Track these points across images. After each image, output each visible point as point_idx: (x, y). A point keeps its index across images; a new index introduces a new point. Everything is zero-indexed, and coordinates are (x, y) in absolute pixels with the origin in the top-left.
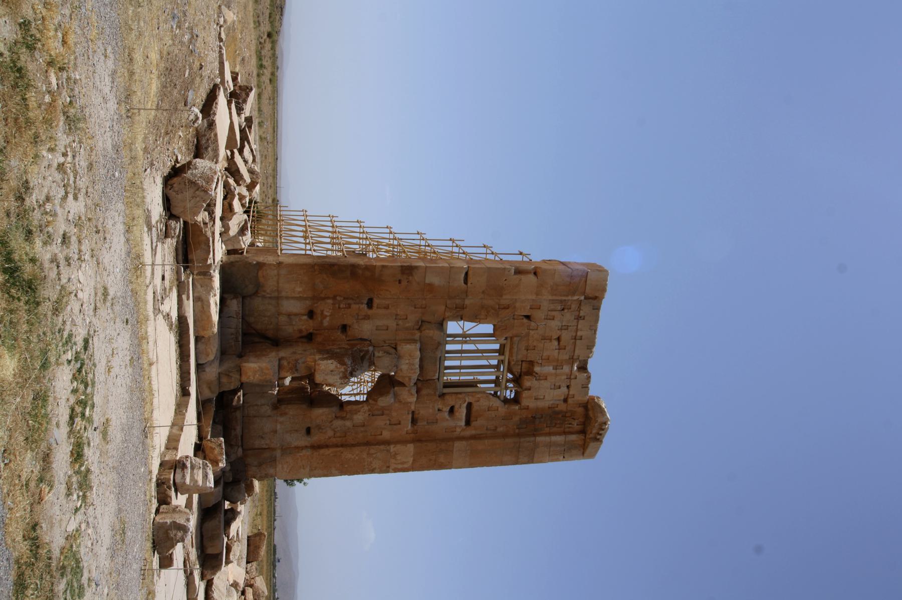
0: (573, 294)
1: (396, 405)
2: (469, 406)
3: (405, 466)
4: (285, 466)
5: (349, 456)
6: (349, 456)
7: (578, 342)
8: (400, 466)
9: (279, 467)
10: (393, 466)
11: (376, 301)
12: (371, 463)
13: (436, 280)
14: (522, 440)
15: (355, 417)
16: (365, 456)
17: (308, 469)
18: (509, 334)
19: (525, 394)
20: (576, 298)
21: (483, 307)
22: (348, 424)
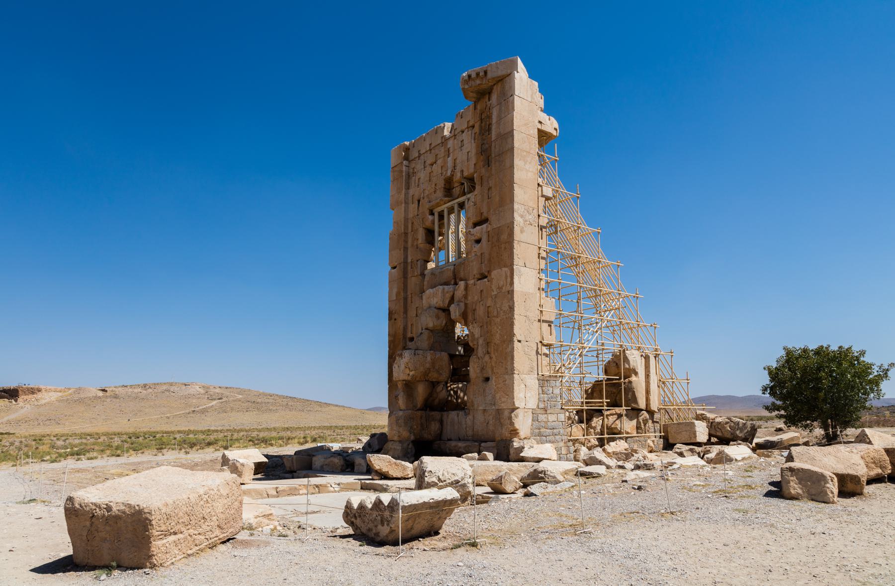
0: (401, 171)
1: (469, 298)
2: (475, 225)
3: (509, 274)
4: (503, 400)
5: (498, 336)
6: (498, 336)
7: (433, 146)
8: (509, 280)
9: (503, 406)
10: (508, 288)
11: (409, 335)
12: (504, 312)
13: (395, 290)
14: (493, 155)
15: (476, 336)
16: (498, 320)
17: (506, 377)
18: (427, 212)
19: (466, 174)
20: (404, 168)
21: (412, 245)
22: (481, 341)
